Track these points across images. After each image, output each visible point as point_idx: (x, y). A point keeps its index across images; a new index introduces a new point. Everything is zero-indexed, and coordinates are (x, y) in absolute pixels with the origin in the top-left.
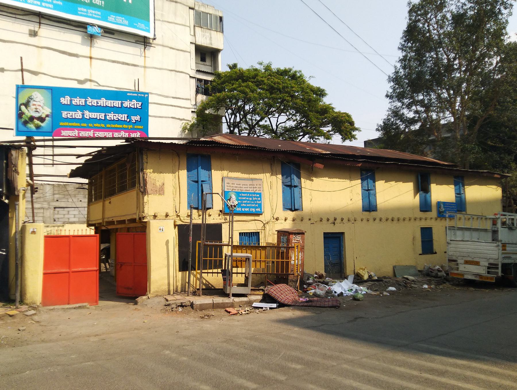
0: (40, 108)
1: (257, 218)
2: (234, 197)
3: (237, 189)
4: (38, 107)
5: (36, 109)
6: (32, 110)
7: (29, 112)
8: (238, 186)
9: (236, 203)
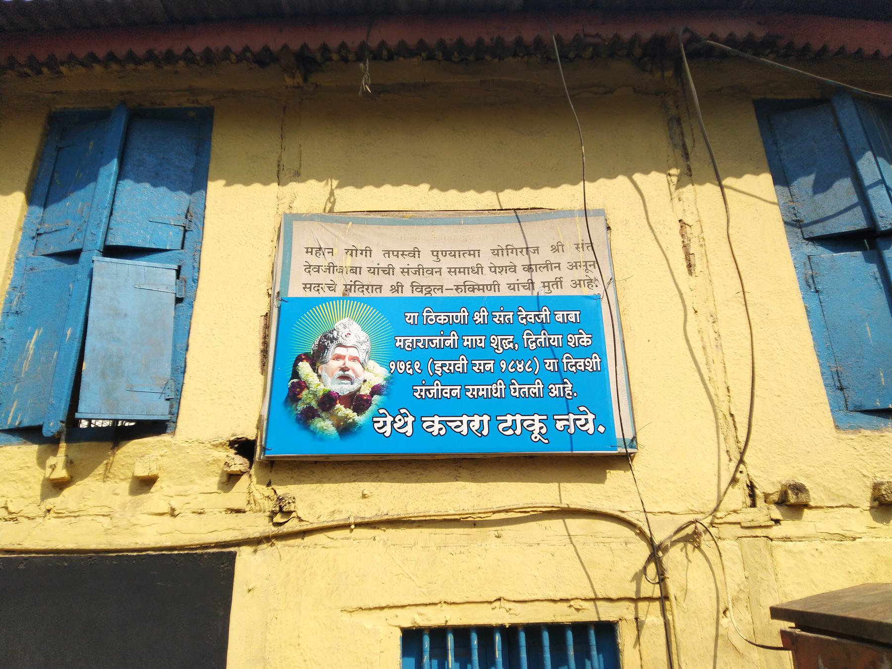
0: (357, 366)
1: (577, 493)
2: (353, 334)
3: (387, 282)
4: (349, 364)
5: (344, 369)
6: (331, 375)
7: (320, 381)
8: (399, 263)
9: (377, 374)
